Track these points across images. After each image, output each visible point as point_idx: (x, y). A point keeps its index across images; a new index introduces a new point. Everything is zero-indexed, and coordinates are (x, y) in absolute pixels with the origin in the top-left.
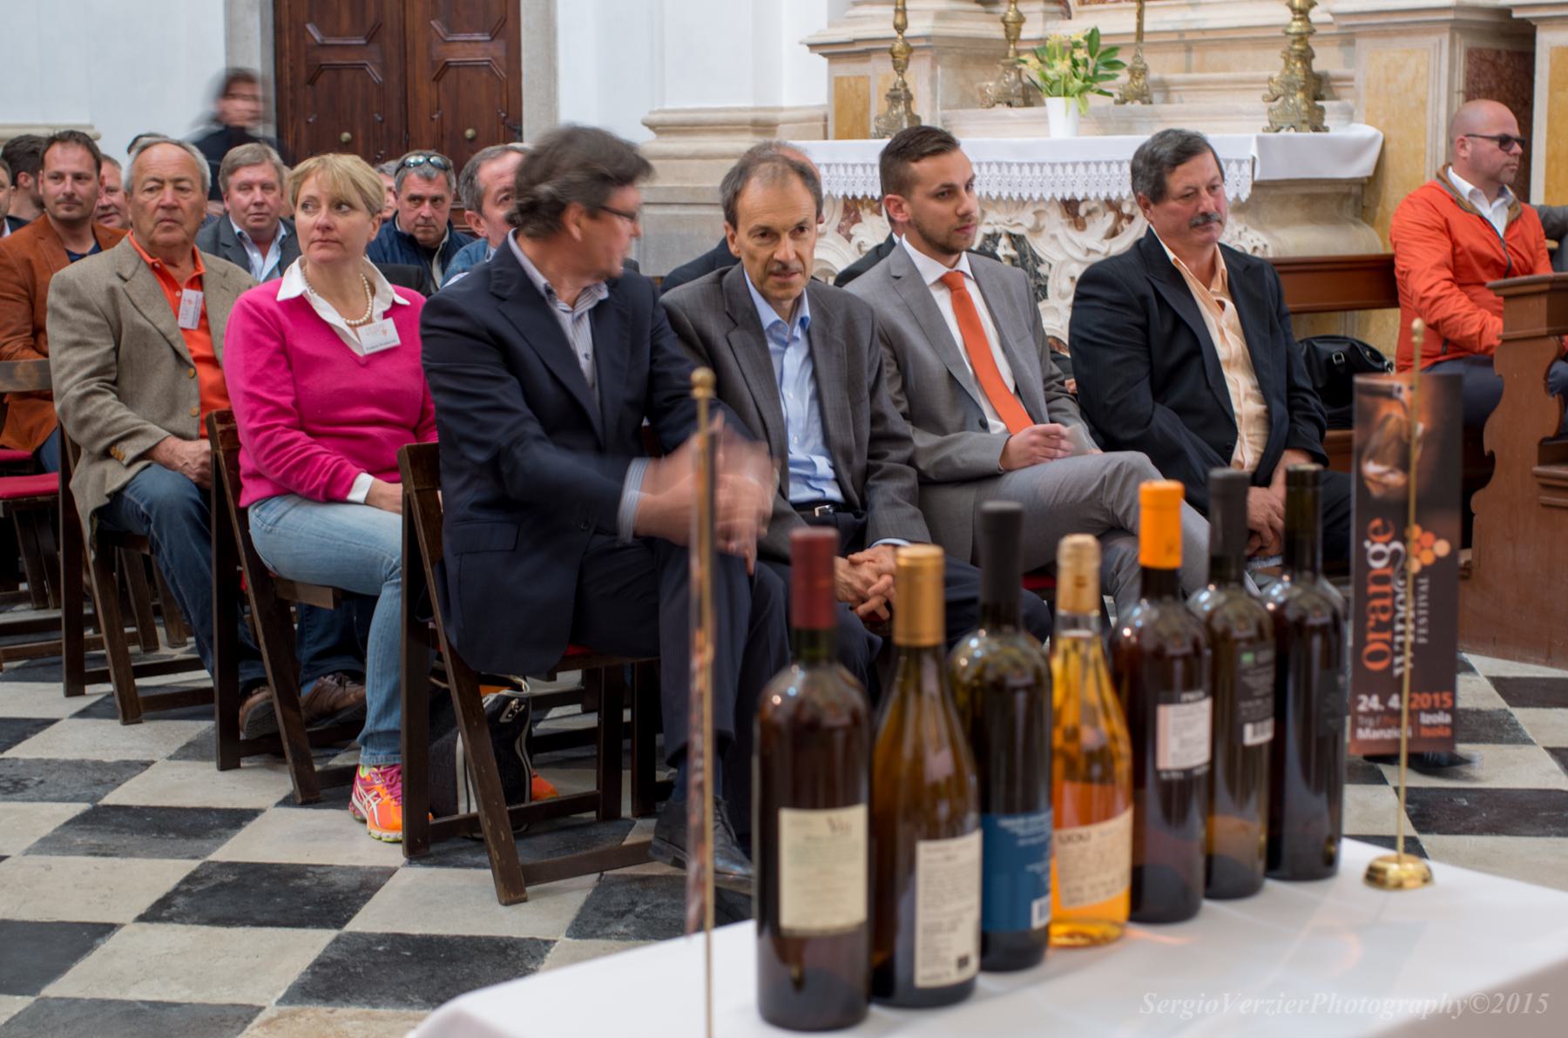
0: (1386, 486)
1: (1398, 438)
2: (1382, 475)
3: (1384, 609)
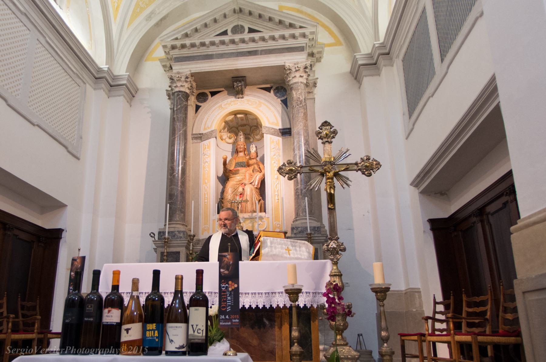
0: (225, 273)
1: (227, 264)
2: (224, 271)
3: (225, 298)
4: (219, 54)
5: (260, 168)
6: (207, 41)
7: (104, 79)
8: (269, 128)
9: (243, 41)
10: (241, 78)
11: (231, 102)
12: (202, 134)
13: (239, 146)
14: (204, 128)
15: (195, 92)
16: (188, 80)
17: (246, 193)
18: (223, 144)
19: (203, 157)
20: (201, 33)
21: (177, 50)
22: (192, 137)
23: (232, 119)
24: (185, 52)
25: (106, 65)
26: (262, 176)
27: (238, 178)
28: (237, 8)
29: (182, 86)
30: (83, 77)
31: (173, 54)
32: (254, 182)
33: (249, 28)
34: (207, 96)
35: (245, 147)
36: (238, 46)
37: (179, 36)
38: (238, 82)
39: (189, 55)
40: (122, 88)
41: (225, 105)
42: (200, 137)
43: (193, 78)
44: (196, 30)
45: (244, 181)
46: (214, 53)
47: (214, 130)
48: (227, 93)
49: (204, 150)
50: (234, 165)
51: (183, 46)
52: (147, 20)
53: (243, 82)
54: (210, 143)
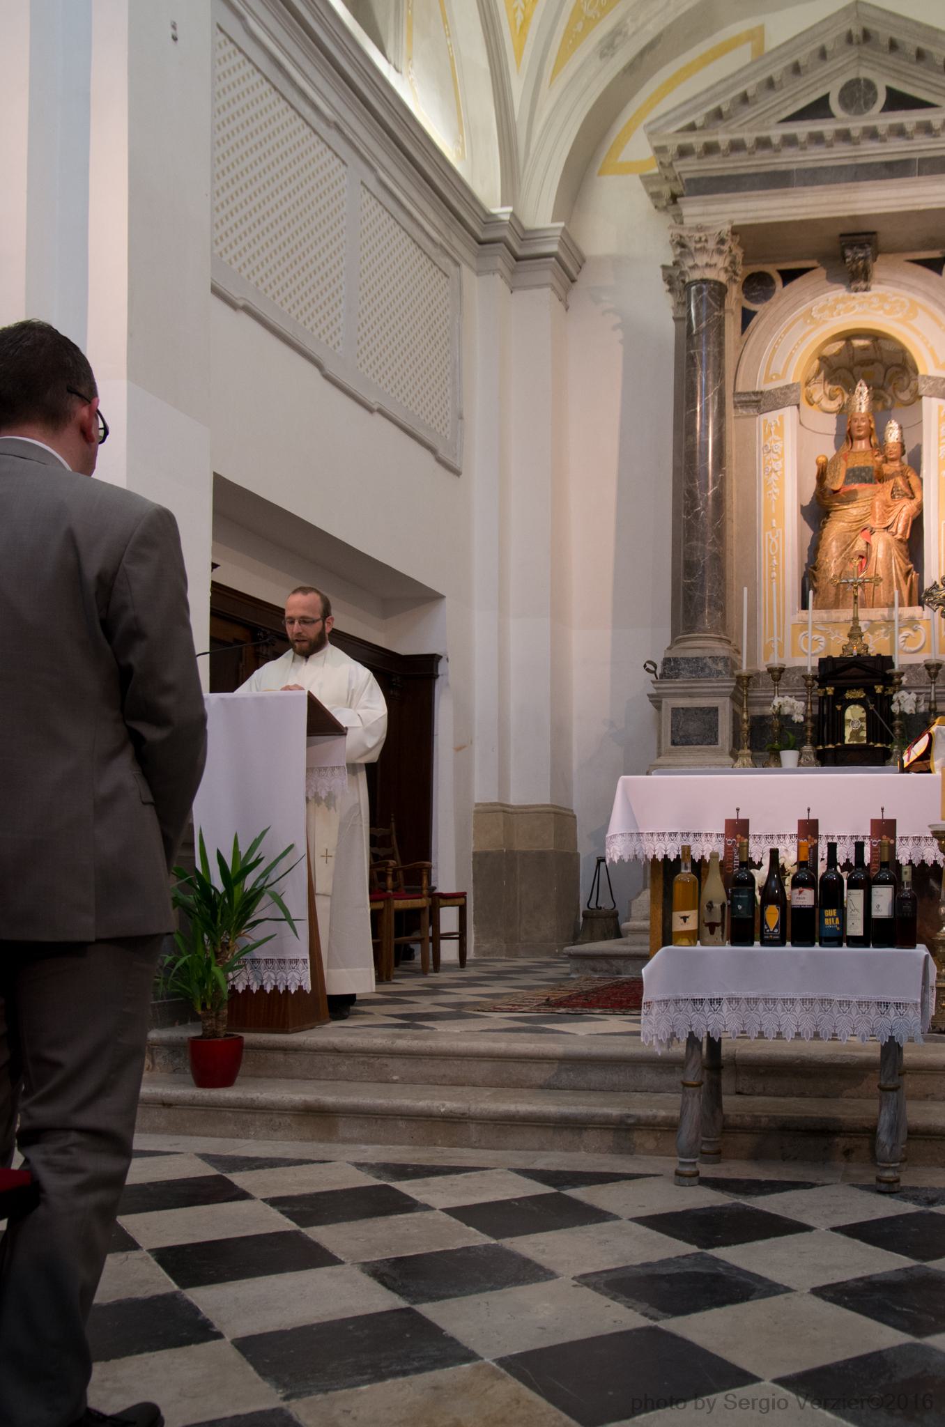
4: (806, 171)
5: (910, 485)
6: (776, 134)
7: (502, 245)
8: (936, 379)
9: (872, 134)
10: (864, 237)
11: (837, 301)
12: (762, 393)
13: (856, 424)
14: (766, 377)
15: (740, 273)
16: (725, 248)
17: (873, 555)
18: (810, 413)
19: (764, 457)
20: (756, 107)
21: (695, 157)
22: (734, 402)
23: (840, 350)
24: (715, 166)
25: (503, 205)
26: (915, 509)
27: (853, 511)
28: (857, 32)
29: (708, 265)
30: (453, 248)
31: (681, 169)
32: (895, 525)
33: (890, 91)
34: (772, 282)
35: (872, 426)
36: (857, 147)
37: (698, 118)
38: (855, 248)
39: (726, 173)
40: (546, 263)
41: (821, 310)
42: (758, 402)
43: (738, 238)
44: (745, 99)
45: (868, 522)
46: (794, 167)
47: (793, 385)
48: (825, 276)
49: (766, 439)
50: (842, 478)
51: (710, 149)
52: (602, 55)
53: (869, 249)
54: (781, 418)
